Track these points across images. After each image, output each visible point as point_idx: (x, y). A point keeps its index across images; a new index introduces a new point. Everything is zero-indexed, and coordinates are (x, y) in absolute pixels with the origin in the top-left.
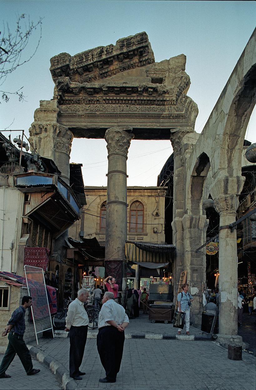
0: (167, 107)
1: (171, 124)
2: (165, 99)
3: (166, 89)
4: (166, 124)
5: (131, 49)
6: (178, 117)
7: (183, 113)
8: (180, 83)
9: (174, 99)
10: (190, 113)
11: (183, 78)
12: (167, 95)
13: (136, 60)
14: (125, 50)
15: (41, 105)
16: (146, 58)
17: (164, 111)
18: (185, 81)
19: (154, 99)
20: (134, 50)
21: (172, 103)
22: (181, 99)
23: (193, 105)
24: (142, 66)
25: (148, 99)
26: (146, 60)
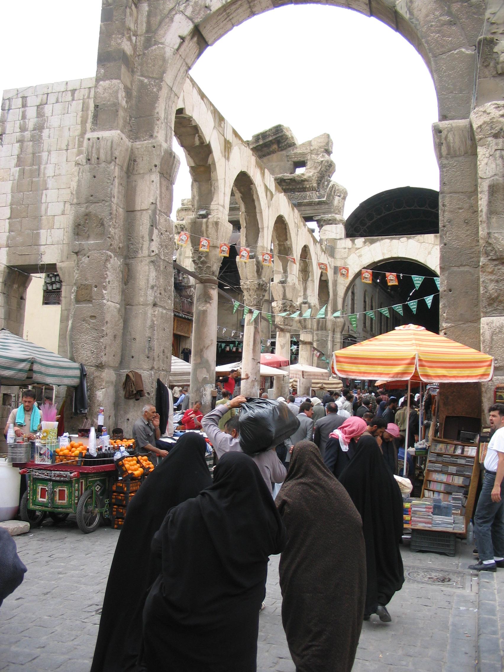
0: (308, 193)
1: (315, 211)
2: (304, 186)
3: (305, 177)
4: (308, 212)
5: (267, 140)
6: (320, 203)
7: (324, 199)
8: (320, 168)
9: (315, 185)
10: (333, 198)
11: (324, 162)
12: (306, 183)
13: (275, 146)
14: (261, 142)
15: (183, 204)
16: (285, 143)
17: (305, 198)
18: (326, 164)
19: (294, 187)
20: (271, 141)
21: (313, 189)
22: (324, 183)
23: (337, 188)
24: (282, 150)
25: (287, 187)
26: (285, 145)
